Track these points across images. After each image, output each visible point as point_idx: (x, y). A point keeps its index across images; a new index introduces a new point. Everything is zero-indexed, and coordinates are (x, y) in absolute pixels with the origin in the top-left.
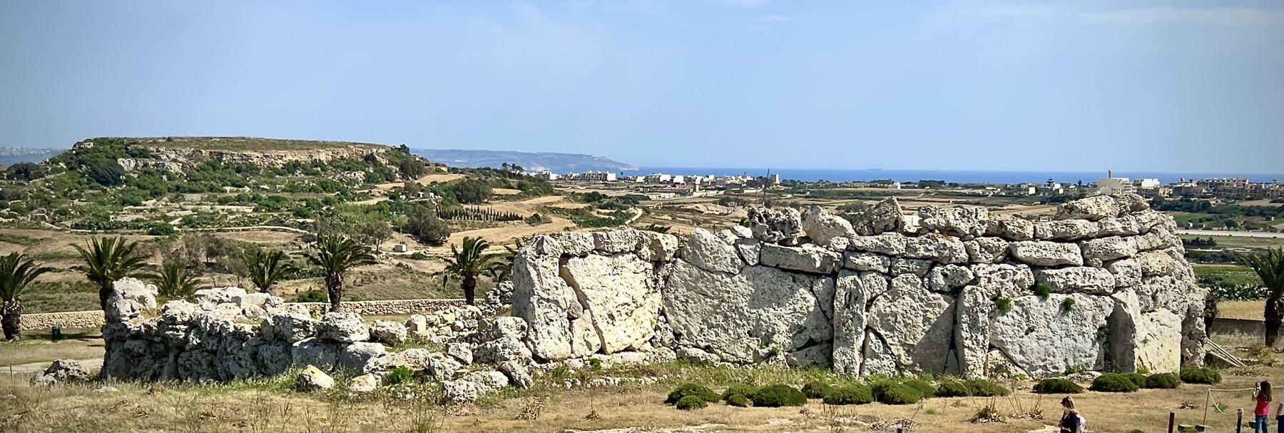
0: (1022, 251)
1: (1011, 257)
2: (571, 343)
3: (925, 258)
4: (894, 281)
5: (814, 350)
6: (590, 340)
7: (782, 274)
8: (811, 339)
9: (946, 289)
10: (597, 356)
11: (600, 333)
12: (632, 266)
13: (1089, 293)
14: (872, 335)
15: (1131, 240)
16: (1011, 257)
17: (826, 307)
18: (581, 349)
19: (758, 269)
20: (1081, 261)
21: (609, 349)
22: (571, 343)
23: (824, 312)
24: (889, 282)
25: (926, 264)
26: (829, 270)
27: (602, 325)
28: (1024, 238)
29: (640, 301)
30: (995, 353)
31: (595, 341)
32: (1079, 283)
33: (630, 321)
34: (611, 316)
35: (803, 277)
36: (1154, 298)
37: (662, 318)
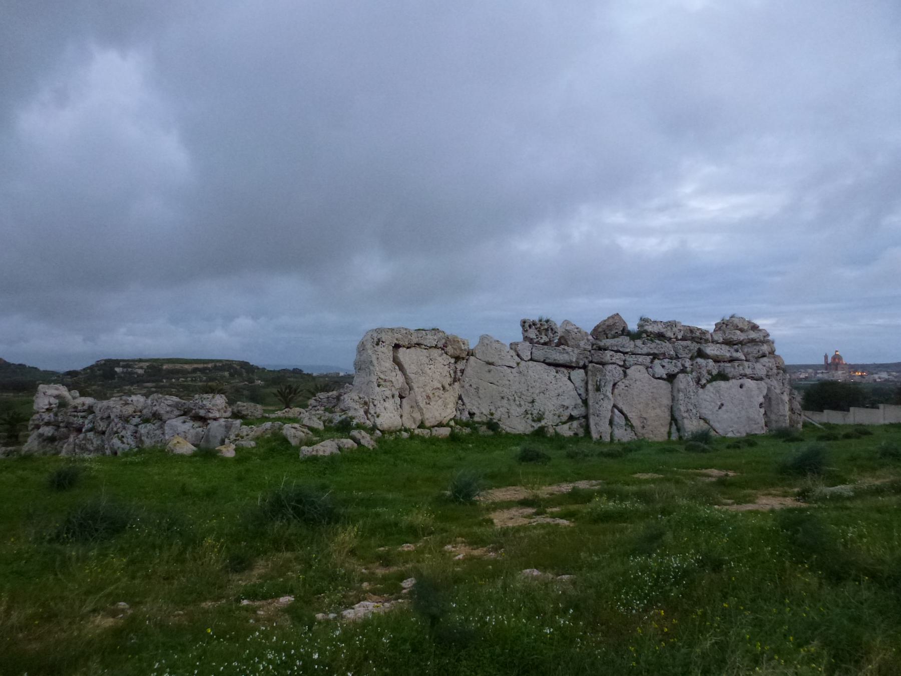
0: (711, 350)
1: (701, 354)
3: (648, 354)
4: (628, 371)
5: (575, 424)
7: (547, 367)
9: (665, 376)
11: (420, 410)
12: (440, 359)
13: (753, 378)
14: (616, 411)
16: (701, 354)
17: (582, 391)
19: (531, 362)
21: (428, 424)
22: (401, 416)
23: (580, 395)
24: (625, 372)
25: (649, 358)
26: (581, 364)
28: (707, 341)
29: (447, 386)
31: (418, 416)
33: (440, 402)
34: (428, 397)
35: (563, 369)
37: (460, 402)
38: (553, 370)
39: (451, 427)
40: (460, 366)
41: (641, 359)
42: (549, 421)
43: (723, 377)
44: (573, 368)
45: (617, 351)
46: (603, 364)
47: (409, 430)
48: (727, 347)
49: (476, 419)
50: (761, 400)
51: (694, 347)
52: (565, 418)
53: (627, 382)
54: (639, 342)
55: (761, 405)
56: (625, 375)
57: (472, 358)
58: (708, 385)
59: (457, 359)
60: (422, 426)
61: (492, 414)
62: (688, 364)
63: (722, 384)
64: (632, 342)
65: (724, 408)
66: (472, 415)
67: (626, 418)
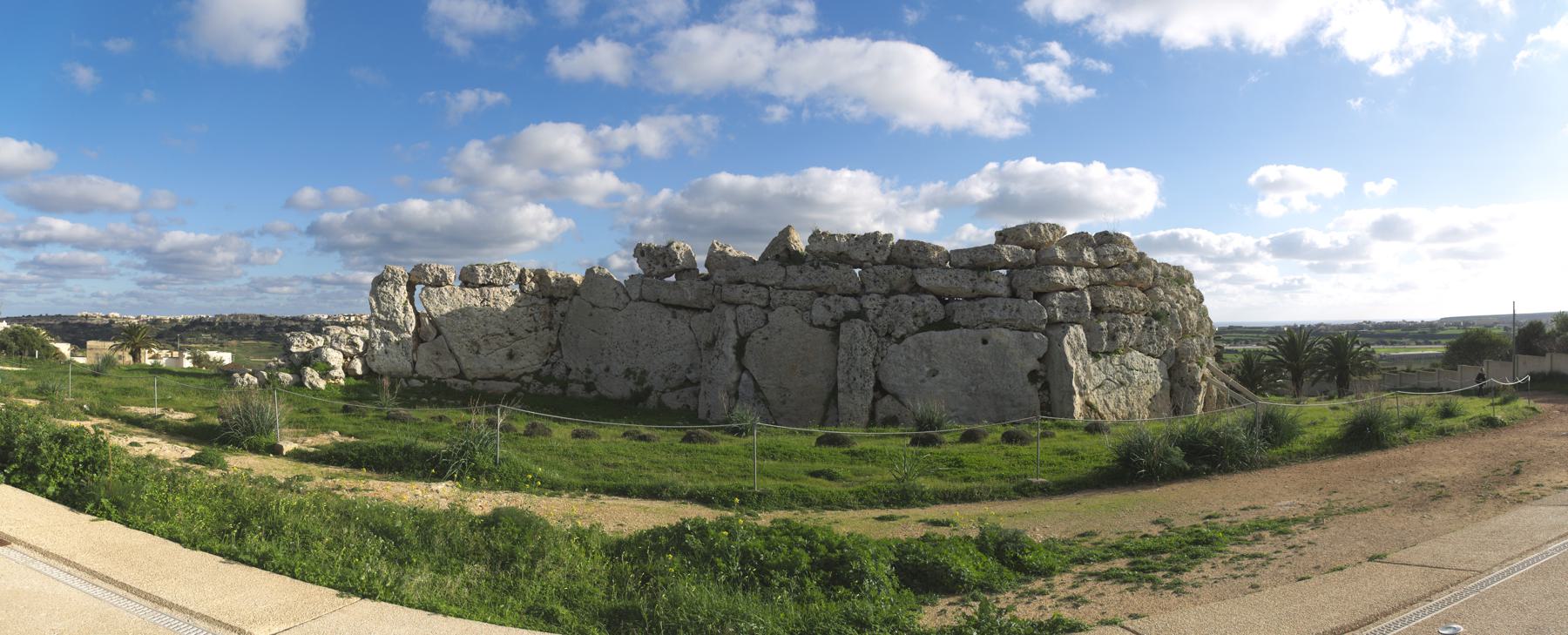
0: (923, 280)
1: (916, 289)
2: (414, 363)
4: (771, 316)
6: (441, 363)
8: (687, 380)
10: (453, 381)
13: (1012, 328)
14: (745, 376)
15: (1079, 273)
16: (916, 289)
18: (423, 369)
20: (1004, 290)
21: (469, 374)
22: (414, 363)
27: (462, 351)
30: (887, 400)
32: (996, 316)
34: (475, 343)
35: (680, 312)
36: (1113, 338)
38: (668, 314)
39: (523, 383)
40: (561, 307)
41: (792, 296)
42: (655, 381)
43: (946, 324)
44: (698, 310)
45: (758, 285)
46: (736, 305)
47: (429, 378)
48: (971, 274)
49: (571, 377)
50: (1032, 363)
51: (899, 275)
52: (672, 383)
53: (766, 332)
54: (793, 270)
55: (1033, 376)
56: (767, 321)
57: (576, 298)
58: (909, 340)
59: (553, 300)
60: (461, 375)
61: (589, 371)
62: (871, 303)
63: (939, 335)
64: (782, 270)
65: (938, 377)
66: (569, 370)
67: (757, 388)
